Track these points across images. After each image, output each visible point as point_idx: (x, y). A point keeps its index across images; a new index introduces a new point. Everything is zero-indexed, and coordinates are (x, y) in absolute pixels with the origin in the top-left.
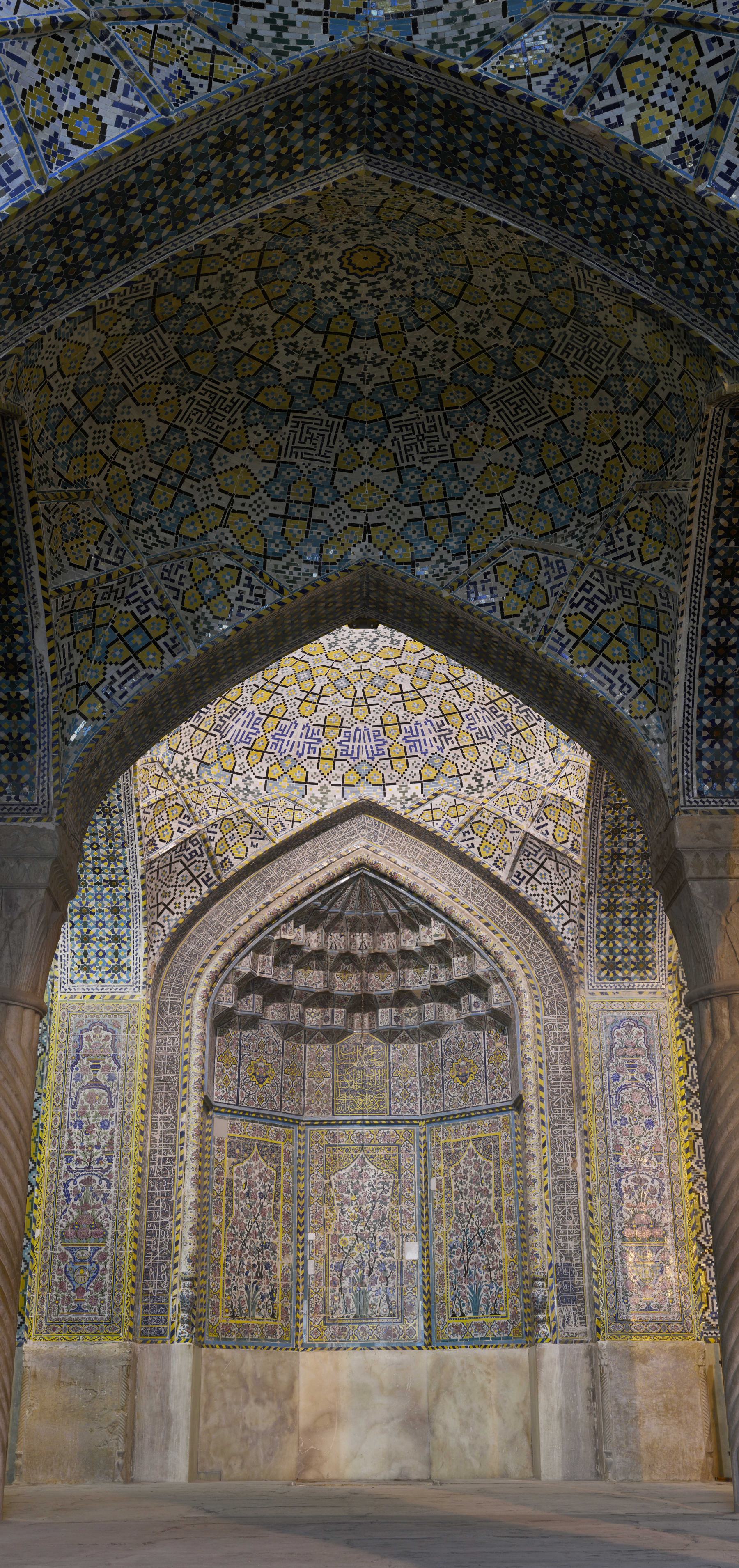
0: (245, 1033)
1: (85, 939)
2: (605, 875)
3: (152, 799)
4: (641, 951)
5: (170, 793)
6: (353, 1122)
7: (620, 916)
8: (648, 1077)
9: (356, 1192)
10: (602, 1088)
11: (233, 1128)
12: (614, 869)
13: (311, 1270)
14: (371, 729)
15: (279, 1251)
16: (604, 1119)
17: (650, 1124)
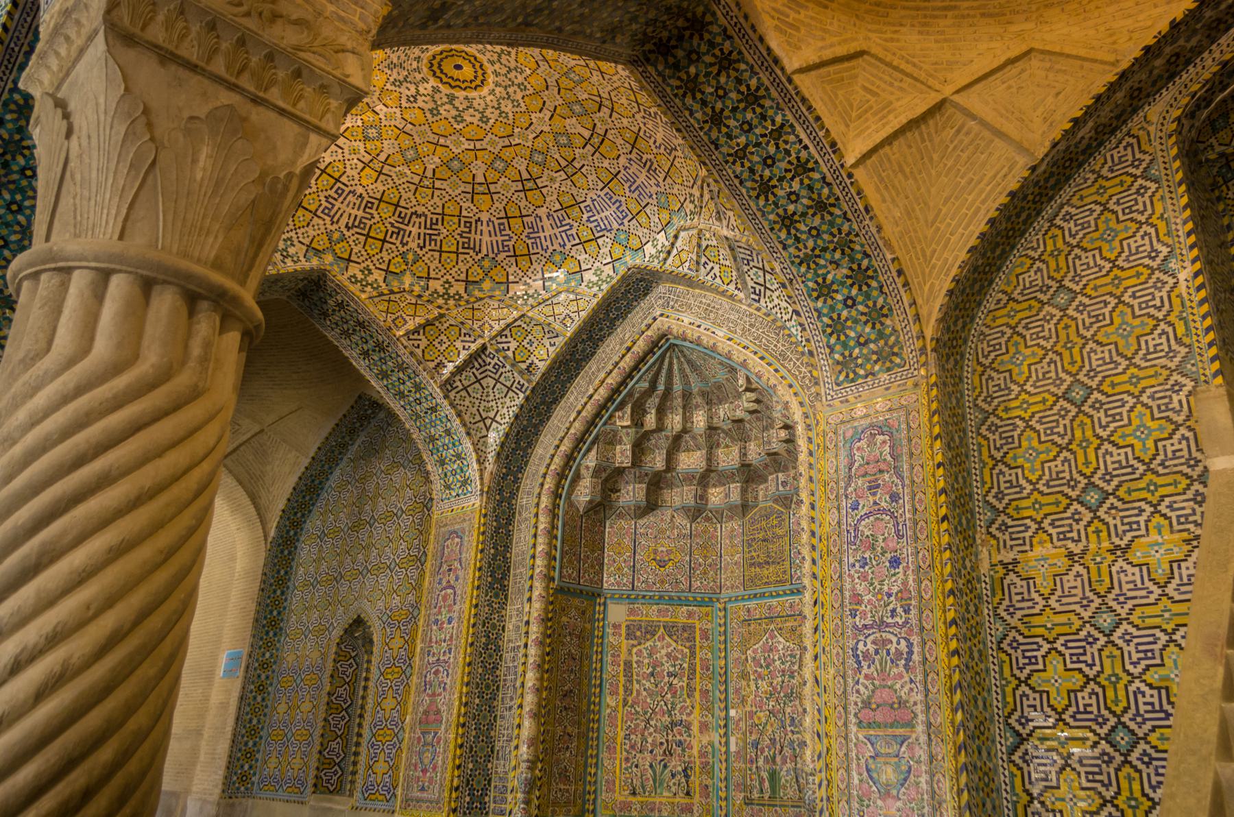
0: (641, 522)
1: (442, 462)
2: (792, 250)
3: (411, 325)
4: (881, 335)
5: (431, 317)
6: (763, 595)
7: (839, 297)
8: (894, 497)
9: (767, 667)
10: (839, 523)
11: (632, 612)
12: (797, 239)
13: (733, 748)
14: (602, 194)
15: (695, 728)
16: (840, 563)
17: (895, 562)
